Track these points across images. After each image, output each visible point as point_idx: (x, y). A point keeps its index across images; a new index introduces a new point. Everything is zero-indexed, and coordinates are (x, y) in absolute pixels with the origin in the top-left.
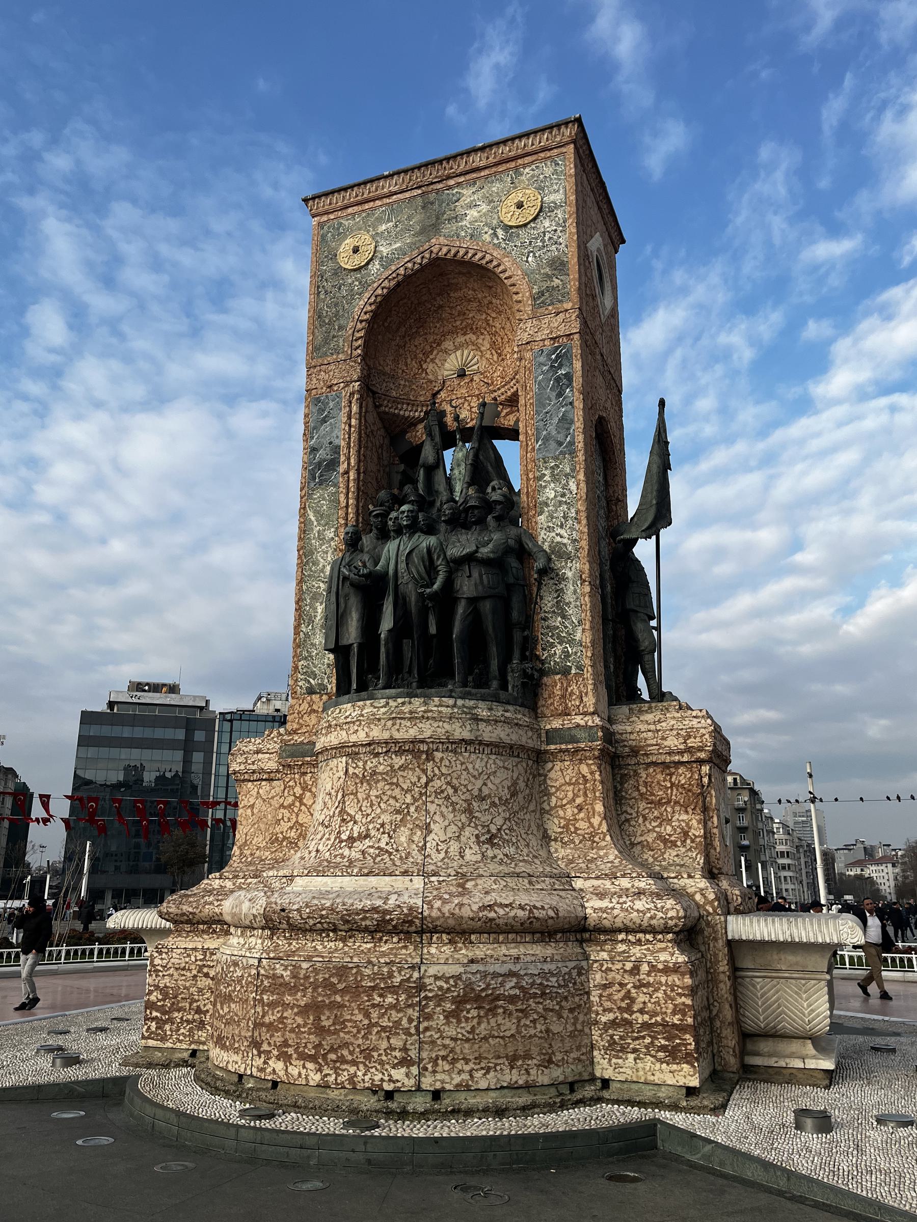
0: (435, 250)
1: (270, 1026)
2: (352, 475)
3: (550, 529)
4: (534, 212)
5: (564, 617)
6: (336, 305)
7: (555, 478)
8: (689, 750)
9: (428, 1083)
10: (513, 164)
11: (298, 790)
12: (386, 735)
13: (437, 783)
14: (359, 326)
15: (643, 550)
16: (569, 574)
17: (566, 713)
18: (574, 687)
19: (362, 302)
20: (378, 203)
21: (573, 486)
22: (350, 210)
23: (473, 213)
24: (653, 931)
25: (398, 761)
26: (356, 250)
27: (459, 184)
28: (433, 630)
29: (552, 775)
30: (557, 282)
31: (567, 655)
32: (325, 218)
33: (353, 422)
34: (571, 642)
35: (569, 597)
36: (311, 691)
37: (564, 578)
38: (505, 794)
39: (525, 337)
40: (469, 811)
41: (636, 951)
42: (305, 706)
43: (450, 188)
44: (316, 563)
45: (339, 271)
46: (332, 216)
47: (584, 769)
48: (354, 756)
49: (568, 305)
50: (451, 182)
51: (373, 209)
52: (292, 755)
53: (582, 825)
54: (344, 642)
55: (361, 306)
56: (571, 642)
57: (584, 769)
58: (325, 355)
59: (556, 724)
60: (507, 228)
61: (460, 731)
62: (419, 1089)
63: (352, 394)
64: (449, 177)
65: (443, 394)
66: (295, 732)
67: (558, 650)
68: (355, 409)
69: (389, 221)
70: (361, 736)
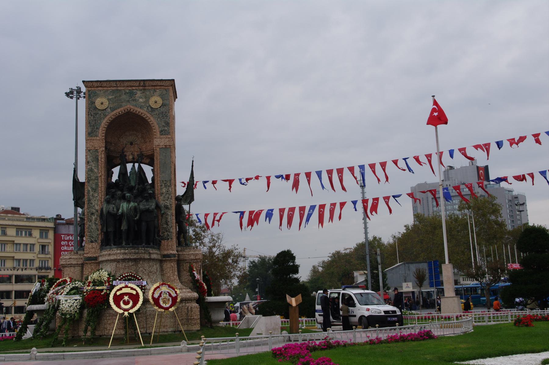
0: (129, 109)
1: (110, 324)
2: (103, 177)
3: (164, 201)
4: (160, 105)
5: (167, 225)
6: (95, 120)
7: (165, 186)
8: (196, 259)
9: (148, 331)
10: (153, 88)
11: (90, 270)
12: (128, 257)
13: (141, 269)
14: (104, 129)
15: (186, 207)
16: (169, 214)
17: (168, 250)
18: (170, 244)
19: (104, 122)
20: (109, 88)
21: (170, 189)
22: (99, 88)
23: (141, 100)
24: (191, 300)
25: (130, 264)
26: (102, 104)
27: (136, 89)
28: (136, 229)
29: (164, 266)
30: (166, 128)
31: (168, 235)
32: (90, 89)
33: (103, 160)
34: (169, 232)
35: (169, 220)
36: (92, 242)
37: (168, 215)
38: (155, 271)
39: (157, 144)
40: (148, 275)
41: (187, 305)
42: (90, 246)
43: (133, 90)
44: (91, 204)
45: (96, 108)
46: (93, 89)
47: (172, 264)
48: (118, 262)
49: (170, 136)
50: (134, 88)
51: (108, 90)
52: (88, 260)
53: (172, 278)
54: (109, 230)
55: (104, 123)
56: (169, 232)
57: (172, 264)
58: (92, 136)
59: (166, 253)
60: (152, 108)
61: (147, 256)
62: (146, 333)
63: (102, 151)
64: (133, 86)
65: (125, 149)
66: (87, 253)
67: (166, 233)
68: (103, 156)
69: (113, 95)
70: (121, 257)
